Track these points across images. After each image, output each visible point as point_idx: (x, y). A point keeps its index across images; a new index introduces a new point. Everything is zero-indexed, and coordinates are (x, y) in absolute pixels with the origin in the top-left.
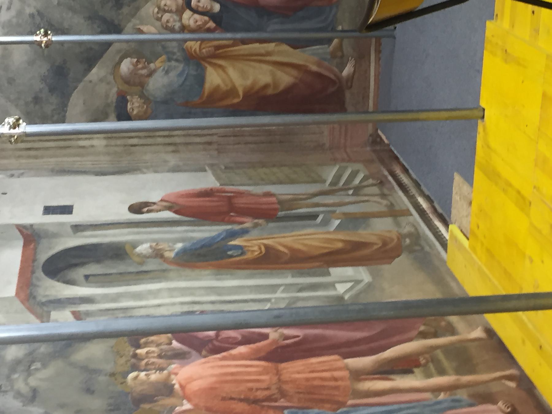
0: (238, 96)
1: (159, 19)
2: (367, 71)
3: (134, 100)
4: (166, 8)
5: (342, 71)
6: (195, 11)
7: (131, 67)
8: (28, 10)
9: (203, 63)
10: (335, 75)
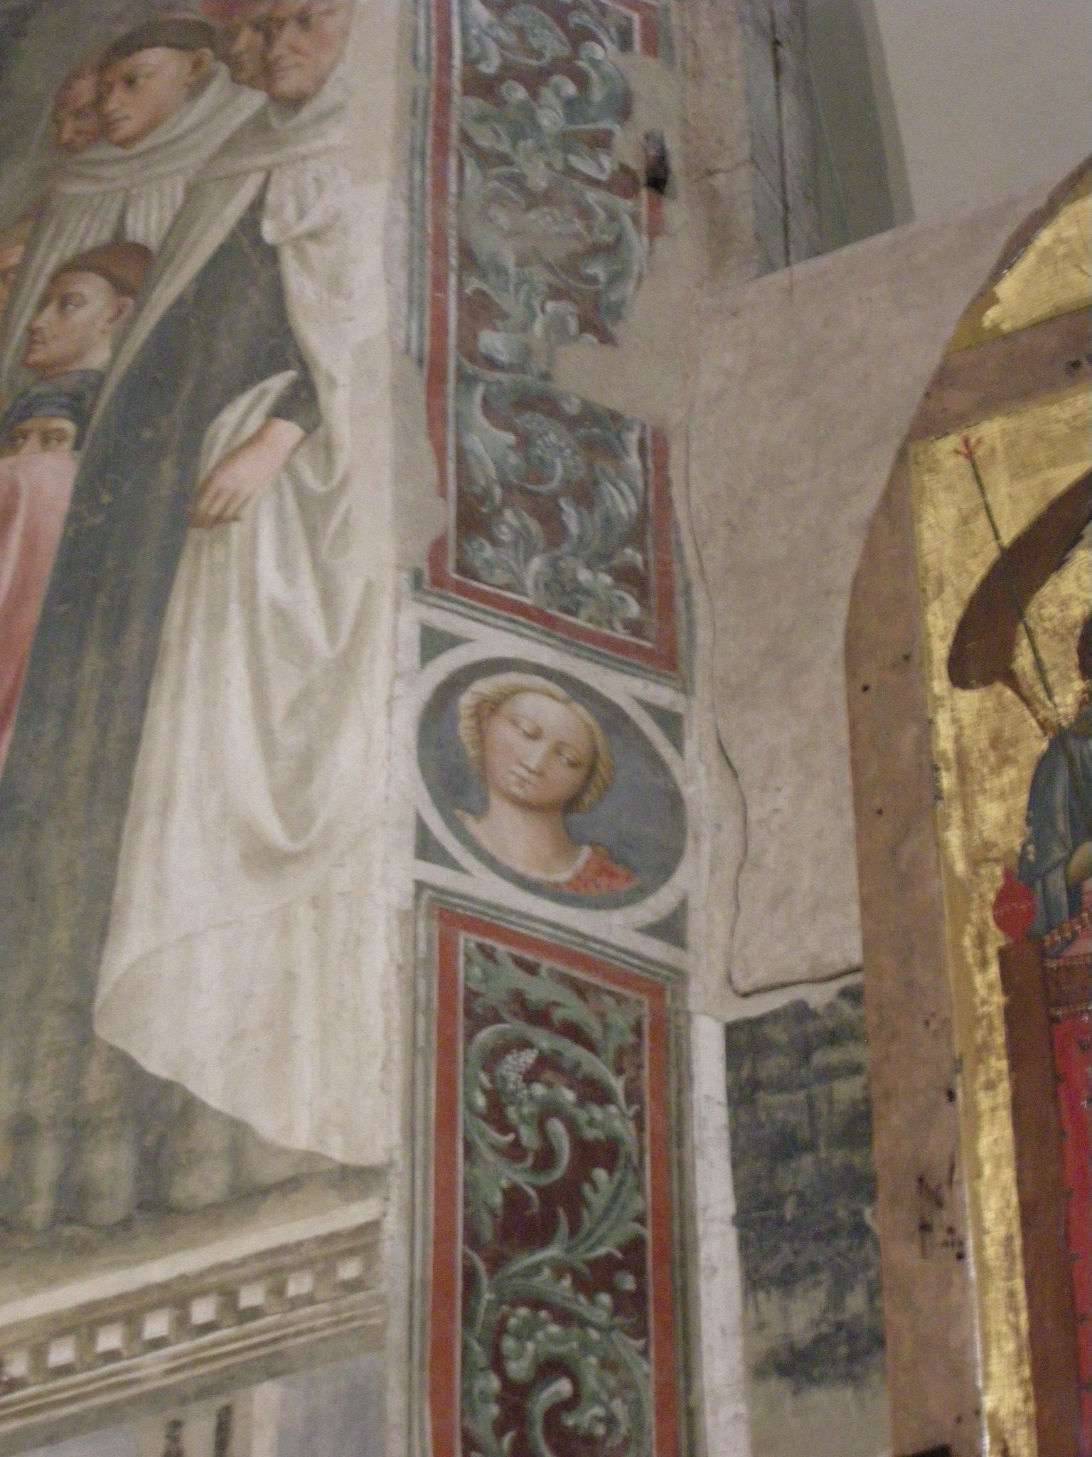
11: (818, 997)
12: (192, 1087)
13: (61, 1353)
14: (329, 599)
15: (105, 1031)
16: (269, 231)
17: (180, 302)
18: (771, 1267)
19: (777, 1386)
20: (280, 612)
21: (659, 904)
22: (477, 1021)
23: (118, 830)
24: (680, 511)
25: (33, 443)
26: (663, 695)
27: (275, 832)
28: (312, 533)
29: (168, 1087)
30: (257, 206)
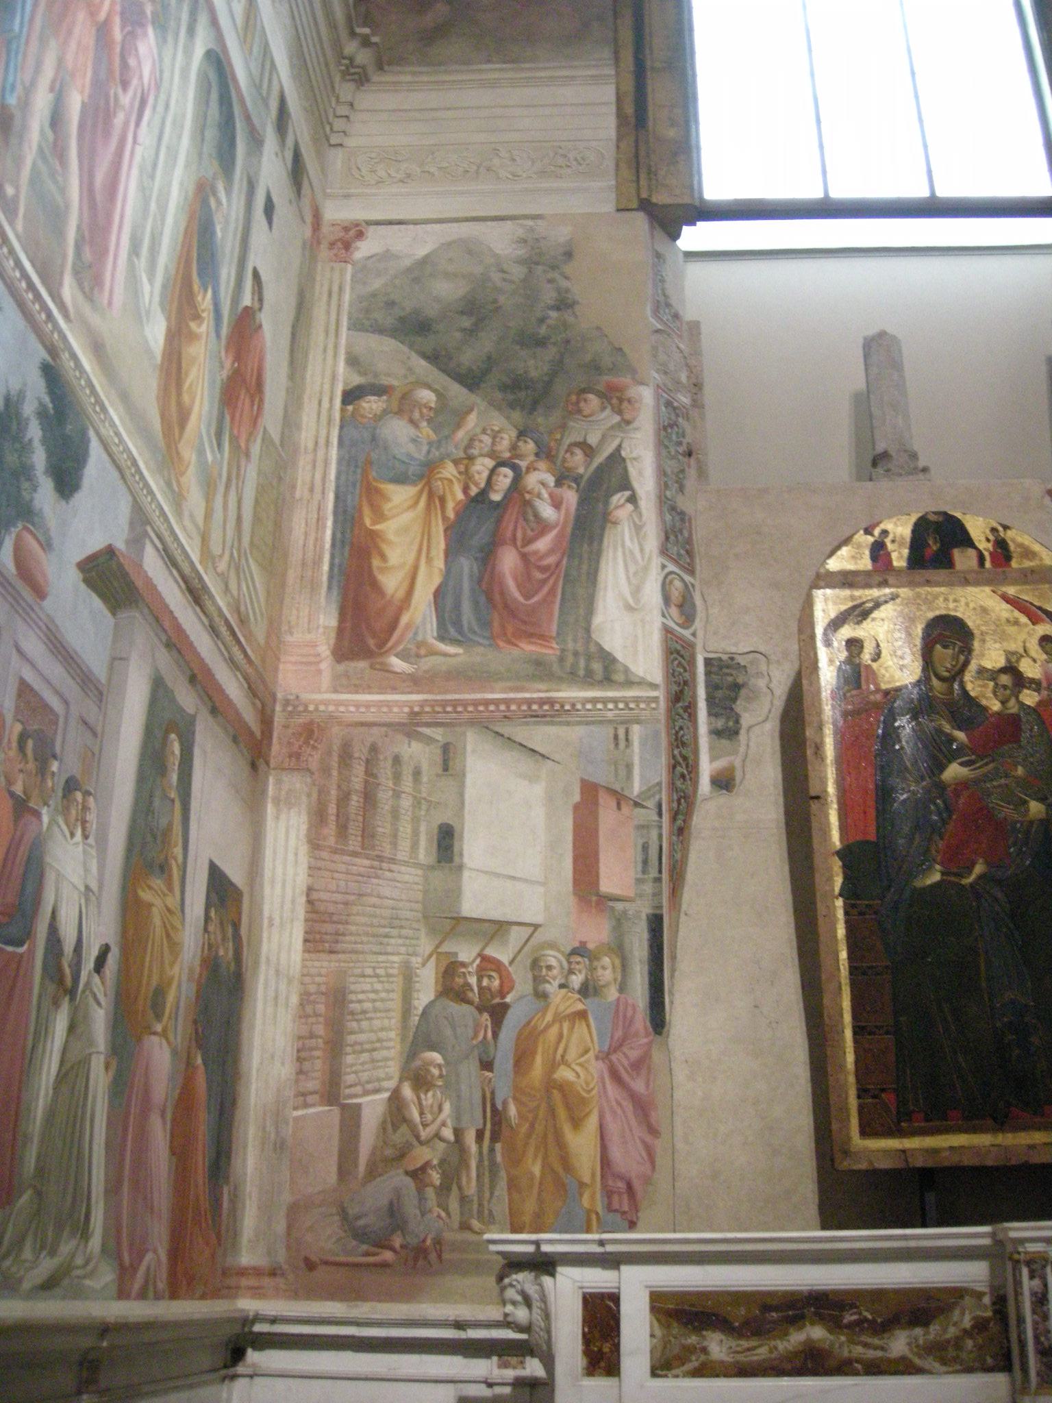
0: (374, 523)
1: (484, 431)
2: (394, 689)
3: (380, 404)
4: (498, 440)
5: (397, 656)
6: (493, 472)
7: (424, 401)
8: (502, 299)
9: (424, 482)
10: (391, 648)
11: (725, 657)
12: (615, 655)
13: (589, 706)
14: (642, 550)
15: (594, 636)
16: (623, 454)
17: (601, 464)
18: (714, 711)
19: (713, 736)
20: (630, 551)
21: (691, 630)
22: (672, 653)
23: (594, 591)
24: (694, 537)
25: (565, 487)
26: (692, 580)
27: (631, 601)
28: (638, 534)
29: (609, 654)
30: (619, 447)
